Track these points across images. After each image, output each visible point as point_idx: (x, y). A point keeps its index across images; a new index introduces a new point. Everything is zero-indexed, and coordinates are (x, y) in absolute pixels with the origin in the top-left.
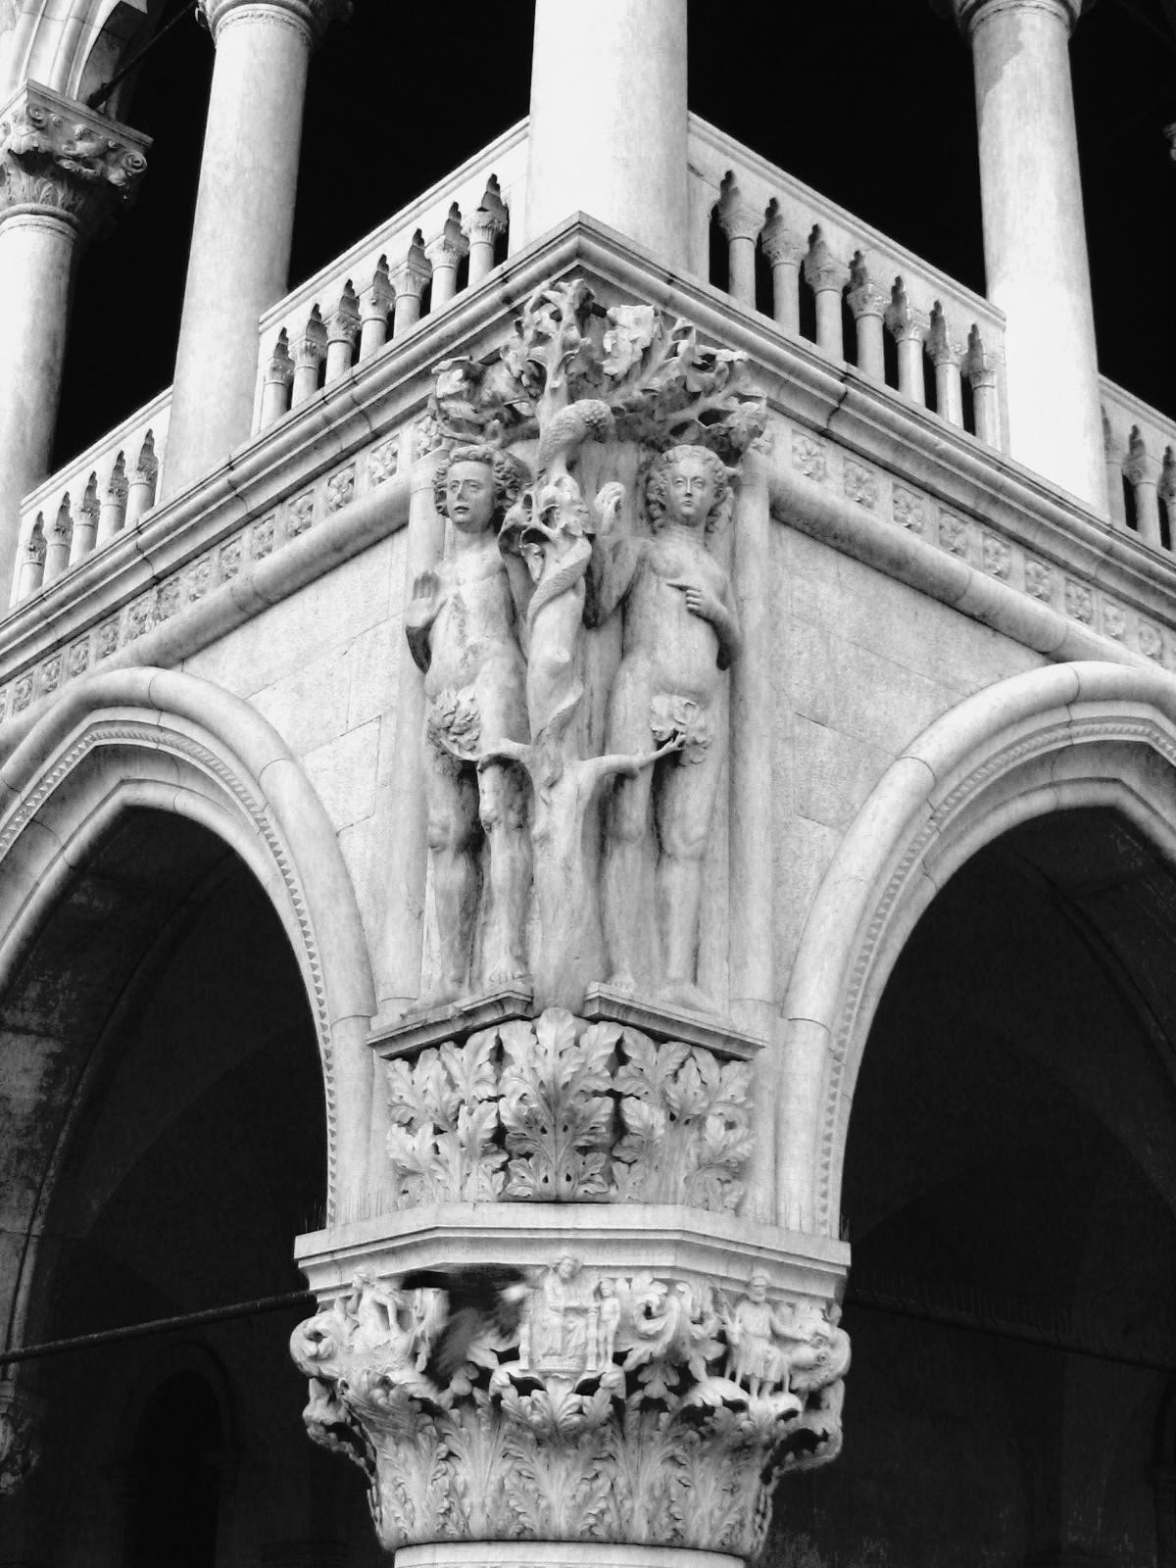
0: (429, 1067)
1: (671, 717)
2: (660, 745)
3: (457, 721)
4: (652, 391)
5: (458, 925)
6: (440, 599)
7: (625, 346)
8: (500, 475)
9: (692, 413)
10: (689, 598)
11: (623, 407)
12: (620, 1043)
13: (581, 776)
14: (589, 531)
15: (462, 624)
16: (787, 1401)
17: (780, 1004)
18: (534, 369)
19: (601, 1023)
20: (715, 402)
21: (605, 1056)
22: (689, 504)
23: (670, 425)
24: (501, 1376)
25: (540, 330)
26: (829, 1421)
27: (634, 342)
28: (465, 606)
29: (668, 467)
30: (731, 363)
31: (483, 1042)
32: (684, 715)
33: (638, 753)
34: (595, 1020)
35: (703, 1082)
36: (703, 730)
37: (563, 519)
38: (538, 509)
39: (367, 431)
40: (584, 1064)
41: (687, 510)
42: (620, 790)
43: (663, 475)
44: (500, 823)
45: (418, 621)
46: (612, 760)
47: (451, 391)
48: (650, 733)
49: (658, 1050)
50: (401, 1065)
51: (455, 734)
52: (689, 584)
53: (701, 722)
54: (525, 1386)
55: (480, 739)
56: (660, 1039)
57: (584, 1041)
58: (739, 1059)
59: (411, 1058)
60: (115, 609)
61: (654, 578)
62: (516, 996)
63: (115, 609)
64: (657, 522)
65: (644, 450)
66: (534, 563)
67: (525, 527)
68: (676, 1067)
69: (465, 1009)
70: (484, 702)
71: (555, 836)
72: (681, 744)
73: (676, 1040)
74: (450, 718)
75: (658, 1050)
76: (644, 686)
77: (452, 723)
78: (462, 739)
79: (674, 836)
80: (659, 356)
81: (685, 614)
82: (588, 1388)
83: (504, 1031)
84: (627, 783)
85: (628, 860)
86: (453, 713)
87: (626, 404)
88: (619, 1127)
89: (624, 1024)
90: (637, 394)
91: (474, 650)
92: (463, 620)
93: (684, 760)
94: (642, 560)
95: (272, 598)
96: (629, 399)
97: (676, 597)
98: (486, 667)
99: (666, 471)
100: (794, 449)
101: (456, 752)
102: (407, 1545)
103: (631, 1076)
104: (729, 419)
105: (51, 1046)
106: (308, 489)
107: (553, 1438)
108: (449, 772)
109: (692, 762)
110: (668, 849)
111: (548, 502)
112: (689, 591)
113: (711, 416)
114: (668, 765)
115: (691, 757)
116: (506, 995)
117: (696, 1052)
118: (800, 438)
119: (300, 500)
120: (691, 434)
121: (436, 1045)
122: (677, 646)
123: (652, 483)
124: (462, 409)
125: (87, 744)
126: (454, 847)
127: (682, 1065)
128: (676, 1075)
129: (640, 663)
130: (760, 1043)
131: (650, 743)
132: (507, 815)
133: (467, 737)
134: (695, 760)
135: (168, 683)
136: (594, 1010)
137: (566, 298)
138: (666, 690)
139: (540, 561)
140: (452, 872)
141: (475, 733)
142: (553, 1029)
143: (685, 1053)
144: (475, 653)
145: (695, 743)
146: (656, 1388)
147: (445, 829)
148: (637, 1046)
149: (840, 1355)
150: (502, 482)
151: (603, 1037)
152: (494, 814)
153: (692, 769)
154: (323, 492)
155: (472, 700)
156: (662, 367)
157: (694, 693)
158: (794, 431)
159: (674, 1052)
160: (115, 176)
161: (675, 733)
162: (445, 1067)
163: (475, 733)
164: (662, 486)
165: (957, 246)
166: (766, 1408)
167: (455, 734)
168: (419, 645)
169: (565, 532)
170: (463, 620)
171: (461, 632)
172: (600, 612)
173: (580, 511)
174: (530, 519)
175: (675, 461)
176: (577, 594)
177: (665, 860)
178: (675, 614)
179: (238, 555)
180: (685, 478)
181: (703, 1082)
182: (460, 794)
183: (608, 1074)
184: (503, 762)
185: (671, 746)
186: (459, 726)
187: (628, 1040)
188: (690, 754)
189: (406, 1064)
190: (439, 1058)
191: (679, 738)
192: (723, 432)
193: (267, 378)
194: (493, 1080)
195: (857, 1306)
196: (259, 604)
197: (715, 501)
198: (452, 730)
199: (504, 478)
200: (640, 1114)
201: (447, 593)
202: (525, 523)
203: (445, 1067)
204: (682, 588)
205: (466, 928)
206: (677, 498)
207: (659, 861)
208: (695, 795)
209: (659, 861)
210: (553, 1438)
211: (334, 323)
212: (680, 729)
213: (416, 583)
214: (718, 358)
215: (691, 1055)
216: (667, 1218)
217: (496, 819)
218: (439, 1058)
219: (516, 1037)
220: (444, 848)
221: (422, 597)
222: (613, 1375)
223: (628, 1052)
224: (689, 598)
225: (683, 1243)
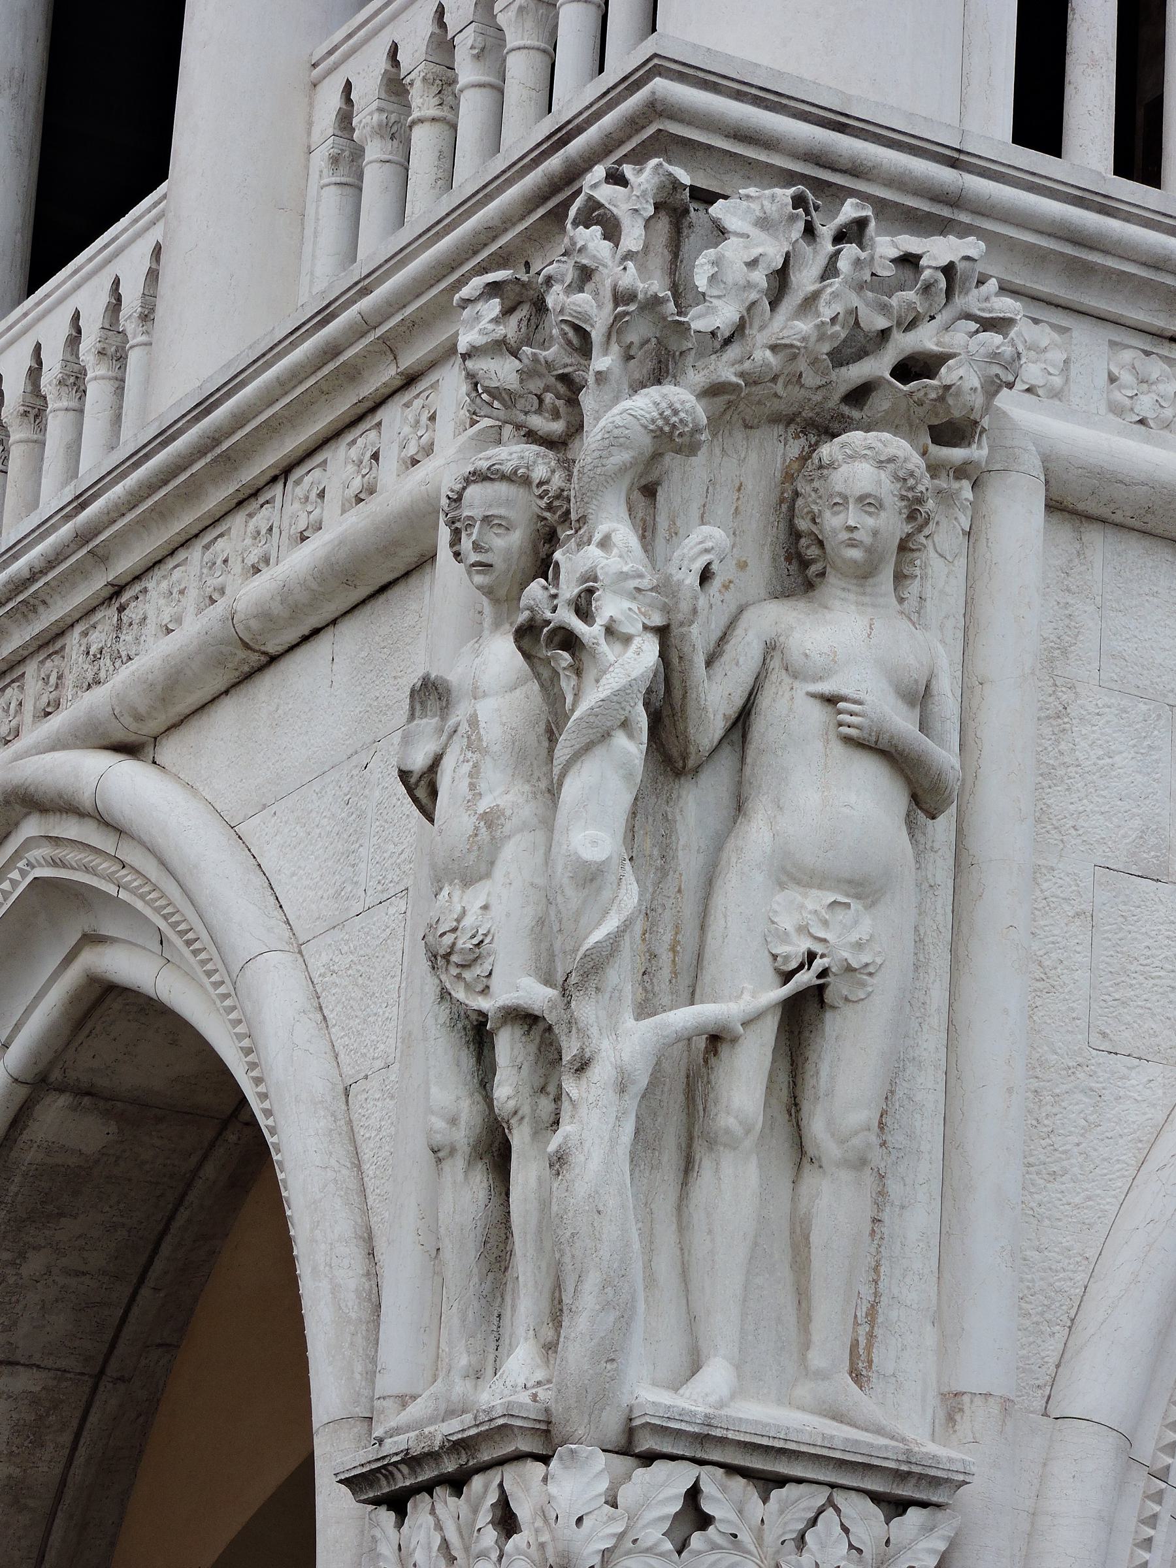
1: (803, 929)
2: (787, 977)
3: (460, 945)
4: (792, 346)
5: (476, 1280)
6: (451, 722)
7: (736, 272)
8: (543, 503)
9: (879, 366)
11: (734, 379)
12: (693, 1494)
14: (657, 620)
18: (571, 334)
19: (659, 1467)
20: (925, 339)
21: (662, 1519)
22: (852, 543)
23: (843, 389)
25: (585, 261)
27: (753, 264)
28: (480, 739)
29: (821, 477)
30: (948, 270)
32: (825, 923)
33: (745, 994)
34: (648, 1459)
35: (851, 1546)
36: (859, 946)
37: (609, 607)
38: (569, 589)
39: (392, 371)
40: (621, 1536)
41: (855, 554)
42: (713, 1061)
43: (816, 490)
44: (522, 1118)
45: (418, 761)
48: (770, 959)
49: (765, 1500)
50: (387, 1517)
51: (458, 966)
52: (844, 691)
53: (863, 930)
56: (769, 1482)
57: (626, 1495)
58: (924, 1505)
59: (398, 1504)
60: (60, 632)
61: (787, 680)
62: (519, 1423)
63: (60, 632)
64: (813, 569)
65: (797, 437)
66: (567, 684)
67: (548, 622)
68: (801, 1526)
69: (454, 1438)
70: (497, 909)
71: (577, 1158)
72: (819, 976)
73: (800, 1481)
74: (448, 940)
75: (765, 1500)
76: (759, 877)
78: (468, 975)
79: (817, 1127)
80: (805, 279)
81: (838, 749)
83: (510, 1476)
84: (724, 1050)
86: (454, 930)
87: (741, 375)
89: (701, 1462)
90: (763, 356)
91: (490, 819)
93: (829, 996)
94: (771, 648)
95: (272, 648)
96: (747, 365)
97: (817, 714)
98: (508, 852)
99: (816, 484)
100: (1112, 379)
101: (460, 994)
103: (714, 1547)
104: (943, 370)
105: (24, 1381)
106: (318, 459)
108: (460, 1025)
109: (847, 999)
110: (811, 1151)
111: (585, 578)
112: (841, 705)
113: (911, 369)
114: (803, 1013)
115: (845, 992)
116: (501, 1421)
117: (840, 1498)
118: (1127, 356)
119: (309, 479)
120: (880, 403)
121: (428, 1488)
122: (821, 798)
123: (800, 502)
124: (502, 371)
125: (24, 874)
126: (467, 1150)
127: (813, 1522)
128: (801, 1540)
129: (758, 835)
130: (961, 1477)
131: (771, 977)
132: (535, 1106)
133: (478, 970)
134: (852, 997)
135: (125, 783)
136: (647, 1443)
137: (632, 198)
138: (798, 882)
139: (574, 680)
140: (467, 1192)
143: (821, 1500)
144: (489, 825)
145: (849, 969)
147: (453, 1121)
148: (723, 1498)
150: (547, 515)
151: (666, 1486)
152: (511, 1104)
153: (847, 1010)
154: (339, 468)
155: (485, 907)
156: (811, 301)
157: (850, 882)
158: (1112, 344)
159: (795, 1503)
161: (812, 956)
162: (439, 1527)
164: (815, 508)
167: (458, 966)
168: (421, 793)
169: (610, 631)
170: (475, 766)
171: (472, 787)
172: (692, 749)
173: (638, 590)
175: (832, 466)
176: (631, 736)
177: (805, 1161)
178: (819, 745)
179: (225, 561)
180: (845, 498)
181: (851, 1546)
183: (668, 1546)
185: (805, 978)
187: (707, 1487)
188: (837, 988)
189: (392, 1514)
190: (433, 1511)
191: (818, 964)
192: (933, 395)
193: (325, 171)
194: (494, 1555)
196: (255, 659)
197: (908, 529)
198: (455, 958)
199: (549, 508)
201: (459, 714)
202: (548, 615)
203: (439, 1527)
204: (831, 700)
205: (487, 1287)
206: (834, 531)
207: (799, 1166)
208: (849, 1061)
209: (799, 1166)
211: (418, 84)
212: (818, 948)
213: (413, 692)
214: (923, 262)
215: (830, 1502)
217: (516, 1113)
218: (433, 1511)
220: (453, 1151)
221: (424, 715)
223: (707, 1507)
224: (841, 717)
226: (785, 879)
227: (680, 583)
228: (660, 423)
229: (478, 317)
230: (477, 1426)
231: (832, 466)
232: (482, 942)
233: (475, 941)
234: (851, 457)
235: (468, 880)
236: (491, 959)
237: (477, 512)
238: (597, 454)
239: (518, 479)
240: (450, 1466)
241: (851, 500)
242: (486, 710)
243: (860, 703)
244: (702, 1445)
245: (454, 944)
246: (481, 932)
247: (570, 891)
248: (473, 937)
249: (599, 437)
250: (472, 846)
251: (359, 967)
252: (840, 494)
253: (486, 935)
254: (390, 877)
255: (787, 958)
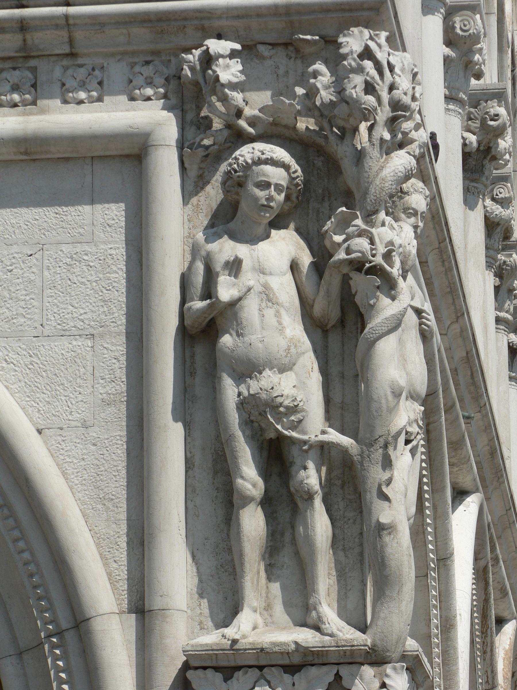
10: (424, 320)
15: (278, 314)
25: (368, 78)
38: (381, 249)
47: (235, 80)
55: (303, 422)
77: (281, 404)
92: (278, 311)
101: (279, 427)
112: (423, 314)
141: (299, 416)
155: (294, 387)
163: (299, 416)
174: (374, 256)
175: (407, 193)
178: (414, 332)
182: (261, 456)
186: (287, 407)
202: (371, 258)
224: (424, 320)
226: (408, 395)
227: (410, 252)
228: (410, 172)
229: (228, 66)
230: (337, 647)
231: (407, 193)
232: (298, 405)
233: (296, 404)
234: (416, 191)
235: (283, 369)
236: (304, 414)
237: (273, 181)
238: (390, 183)
239: (286, 167)
240: (296, 660)
241: (419, 213)
242: (275, 282)
243: (429, 315)
245: (282, 402)
246: (299, 399)
247: (390, 398)
248: (293, 401)
249: (392, 174)
250: (287, 354)
251: (41, 366)
252: (413, 209)
253: (300, 401)
254: (72, 324)
255: (411, 434)
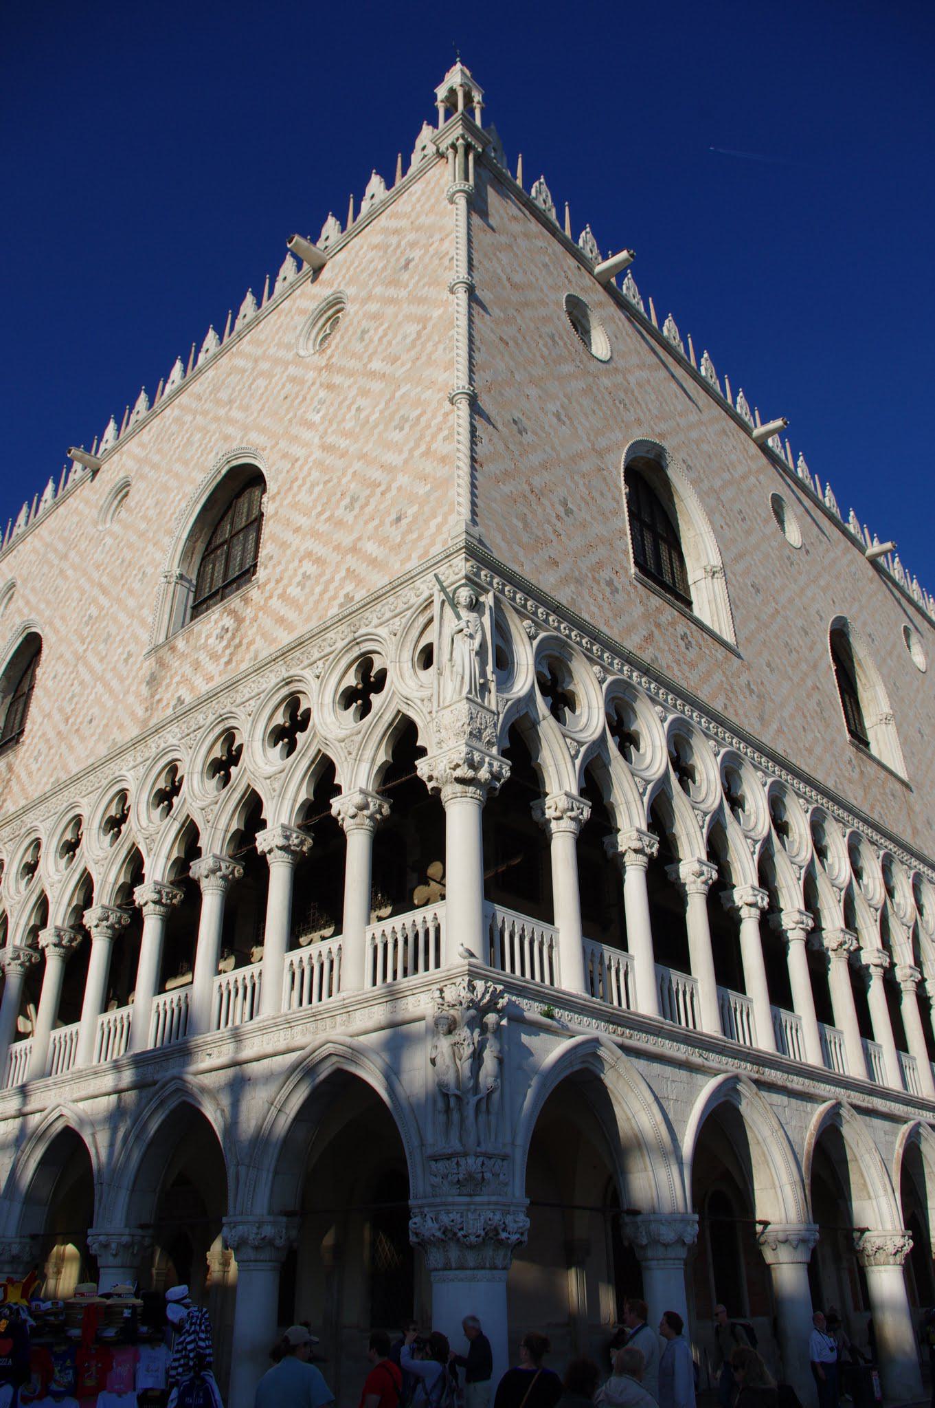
0: (440, 1164)
13: (473, 1100)
16: (518, 1236)
17: (513, 1144)
24: (460, 1234)
26: (525, 1238)
31: (455, 1160)
46: (479, 1096)
54: (465, 1236)
82: (478, 1236)
85: (482, 1118)
88: (483, 1178)
102: (436, 1270)
107: (471, 1247)
140: (442, 1118)
142: (471, 1160)
146: (491, 1235)
149: (528, 1225)
151: (481, 1159)
159: (493, 1161)
160: (305, 849)
165: (547, 915)
166: (514, 1238)
184: (456, 1095)
195: (529, 1213)
200: (488, 1175)
210: (471, 1247)
216: (494, 1199)
219: (462, 1161)
222: (483, 1233)
225: (496, 1204)
244: (485, 1155)
